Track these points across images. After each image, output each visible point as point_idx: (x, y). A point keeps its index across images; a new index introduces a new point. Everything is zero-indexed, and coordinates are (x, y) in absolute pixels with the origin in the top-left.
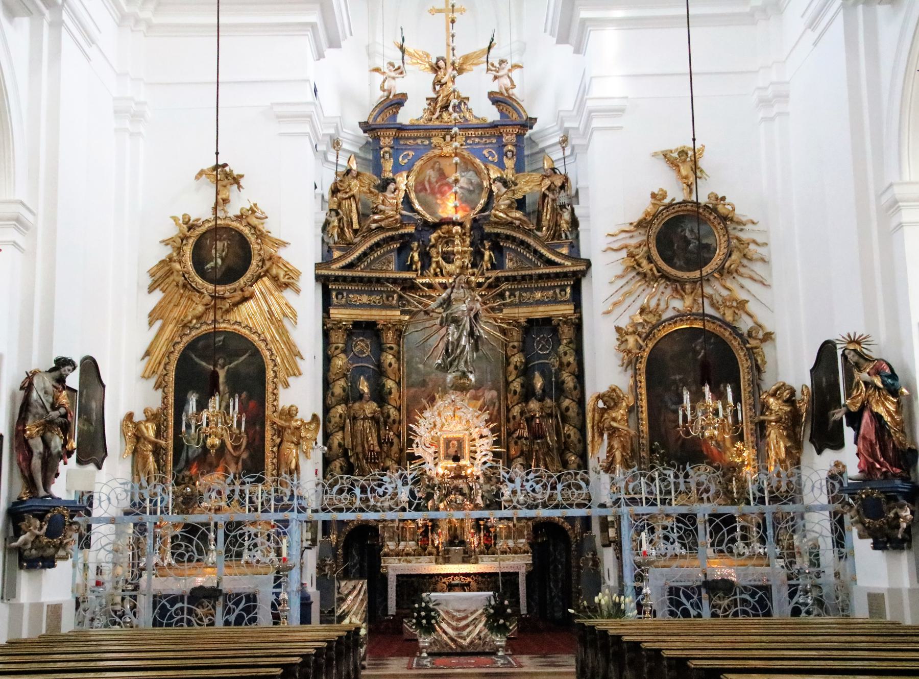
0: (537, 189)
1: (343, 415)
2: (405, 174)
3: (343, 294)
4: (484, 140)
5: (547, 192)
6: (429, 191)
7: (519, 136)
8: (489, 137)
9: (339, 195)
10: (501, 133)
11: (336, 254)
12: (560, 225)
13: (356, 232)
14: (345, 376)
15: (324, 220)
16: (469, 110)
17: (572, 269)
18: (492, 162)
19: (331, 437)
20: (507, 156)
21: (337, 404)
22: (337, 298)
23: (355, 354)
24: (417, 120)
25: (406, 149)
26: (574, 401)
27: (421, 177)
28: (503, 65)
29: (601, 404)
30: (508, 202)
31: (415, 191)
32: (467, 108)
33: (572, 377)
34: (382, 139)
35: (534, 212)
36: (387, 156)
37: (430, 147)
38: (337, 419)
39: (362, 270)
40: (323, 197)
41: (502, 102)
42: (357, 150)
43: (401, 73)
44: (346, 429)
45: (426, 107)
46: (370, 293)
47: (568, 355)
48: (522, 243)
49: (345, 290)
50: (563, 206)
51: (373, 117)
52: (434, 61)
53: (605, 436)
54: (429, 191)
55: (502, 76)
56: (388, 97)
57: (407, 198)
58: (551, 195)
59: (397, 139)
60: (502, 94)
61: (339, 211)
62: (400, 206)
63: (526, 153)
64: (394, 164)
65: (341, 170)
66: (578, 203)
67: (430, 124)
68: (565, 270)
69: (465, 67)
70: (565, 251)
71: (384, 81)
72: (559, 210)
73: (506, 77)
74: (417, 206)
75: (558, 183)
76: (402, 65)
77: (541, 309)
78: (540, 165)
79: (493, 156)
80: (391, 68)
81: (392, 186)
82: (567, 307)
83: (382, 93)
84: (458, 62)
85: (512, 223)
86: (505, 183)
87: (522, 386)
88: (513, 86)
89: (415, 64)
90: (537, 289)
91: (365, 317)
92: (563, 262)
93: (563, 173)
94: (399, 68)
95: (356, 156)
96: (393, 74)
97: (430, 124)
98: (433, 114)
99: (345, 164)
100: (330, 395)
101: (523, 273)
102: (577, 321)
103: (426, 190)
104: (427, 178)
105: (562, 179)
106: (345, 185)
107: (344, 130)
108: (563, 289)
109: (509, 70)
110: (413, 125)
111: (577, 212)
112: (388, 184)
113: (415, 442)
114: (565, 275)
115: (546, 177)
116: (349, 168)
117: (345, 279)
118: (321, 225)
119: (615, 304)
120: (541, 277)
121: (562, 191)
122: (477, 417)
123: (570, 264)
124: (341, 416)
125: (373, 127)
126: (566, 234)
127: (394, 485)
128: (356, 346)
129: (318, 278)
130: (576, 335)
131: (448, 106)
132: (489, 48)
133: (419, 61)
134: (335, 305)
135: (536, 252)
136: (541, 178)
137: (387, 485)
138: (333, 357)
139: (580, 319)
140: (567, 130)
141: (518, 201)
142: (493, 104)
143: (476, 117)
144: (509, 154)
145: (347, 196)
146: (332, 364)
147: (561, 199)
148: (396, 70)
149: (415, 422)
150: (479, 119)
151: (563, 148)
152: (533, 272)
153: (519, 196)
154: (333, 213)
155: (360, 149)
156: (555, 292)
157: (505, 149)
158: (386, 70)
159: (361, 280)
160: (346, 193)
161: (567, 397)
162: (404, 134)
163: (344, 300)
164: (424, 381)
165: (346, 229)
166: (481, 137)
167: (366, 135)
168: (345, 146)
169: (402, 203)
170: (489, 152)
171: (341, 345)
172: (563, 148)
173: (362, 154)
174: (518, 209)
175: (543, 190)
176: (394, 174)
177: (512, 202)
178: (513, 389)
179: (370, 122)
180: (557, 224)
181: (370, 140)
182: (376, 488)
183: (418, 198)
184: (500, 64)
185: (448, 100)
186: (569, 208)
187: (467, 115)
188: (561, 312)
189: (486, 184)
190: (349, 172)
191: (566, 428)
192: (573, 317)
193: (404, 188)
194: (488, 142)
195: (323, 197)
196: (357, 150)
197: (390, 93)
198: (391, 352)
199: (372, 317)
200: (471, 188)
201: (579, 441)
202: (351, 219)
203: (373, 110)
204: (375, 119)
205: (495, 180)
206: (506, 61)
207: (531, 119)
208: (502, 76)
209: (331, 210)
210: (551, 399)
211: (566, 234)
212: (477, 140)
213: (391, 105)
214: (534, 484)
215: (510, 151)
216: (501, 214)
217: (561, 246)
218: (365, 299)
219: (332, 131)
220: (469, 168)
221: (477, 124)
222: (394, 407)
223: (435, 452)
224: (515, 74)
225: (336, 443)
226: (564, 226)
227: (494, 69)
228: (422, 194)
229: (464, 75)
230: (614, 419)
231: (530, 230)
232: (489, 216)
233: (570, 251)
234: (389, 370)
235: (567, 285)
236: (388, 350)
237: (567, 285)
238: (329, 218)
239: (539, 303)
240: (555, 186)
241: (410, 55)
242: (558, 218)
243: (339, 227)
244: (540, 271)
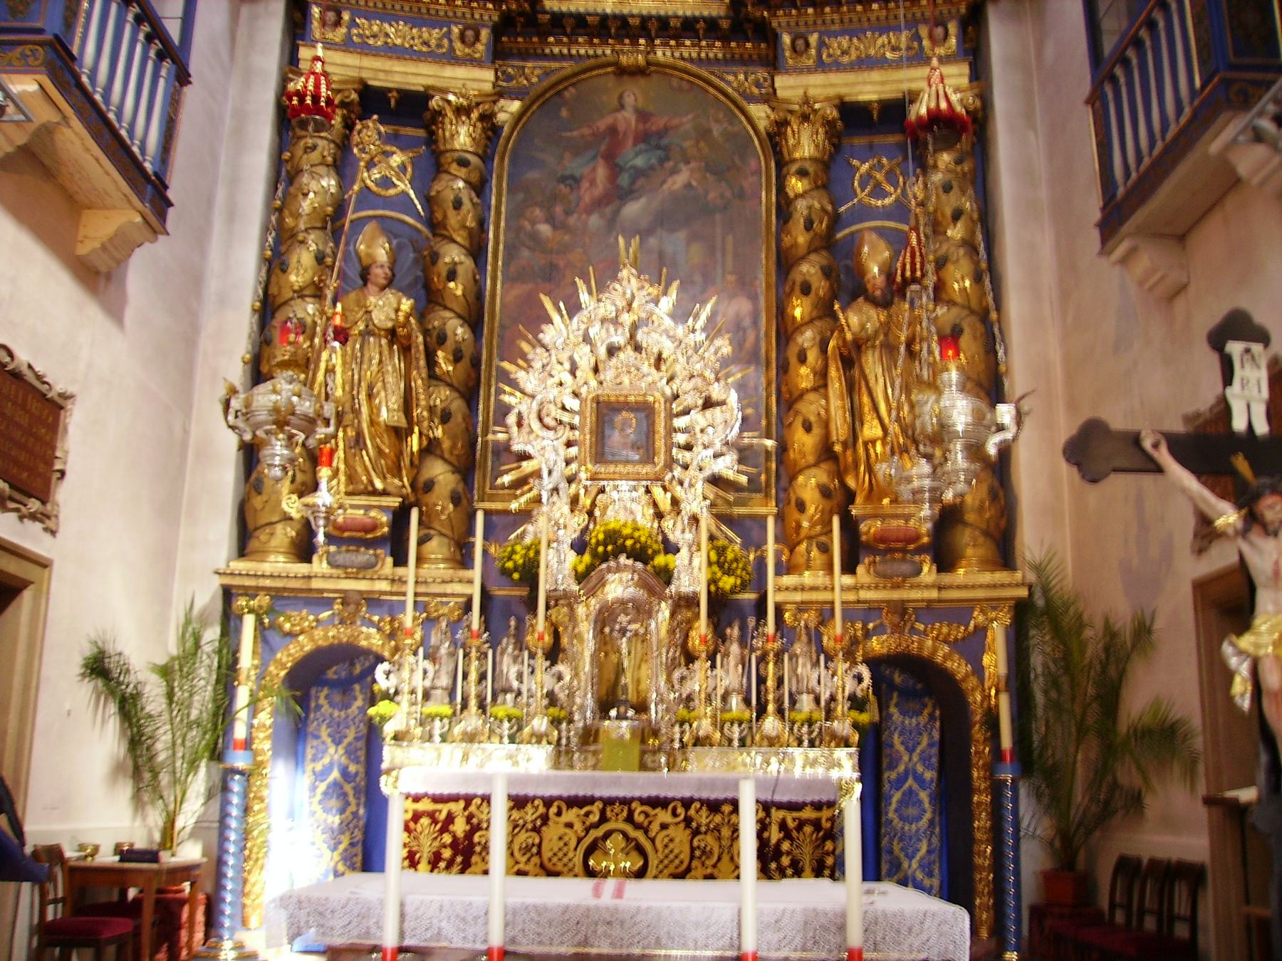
87: (827, 272)
91: (398, 78)
164: (552, 267)
178: (799, 279)
198: (462, 172)
222: (459, 316)
234: (453, 219)
236: (454, 168)
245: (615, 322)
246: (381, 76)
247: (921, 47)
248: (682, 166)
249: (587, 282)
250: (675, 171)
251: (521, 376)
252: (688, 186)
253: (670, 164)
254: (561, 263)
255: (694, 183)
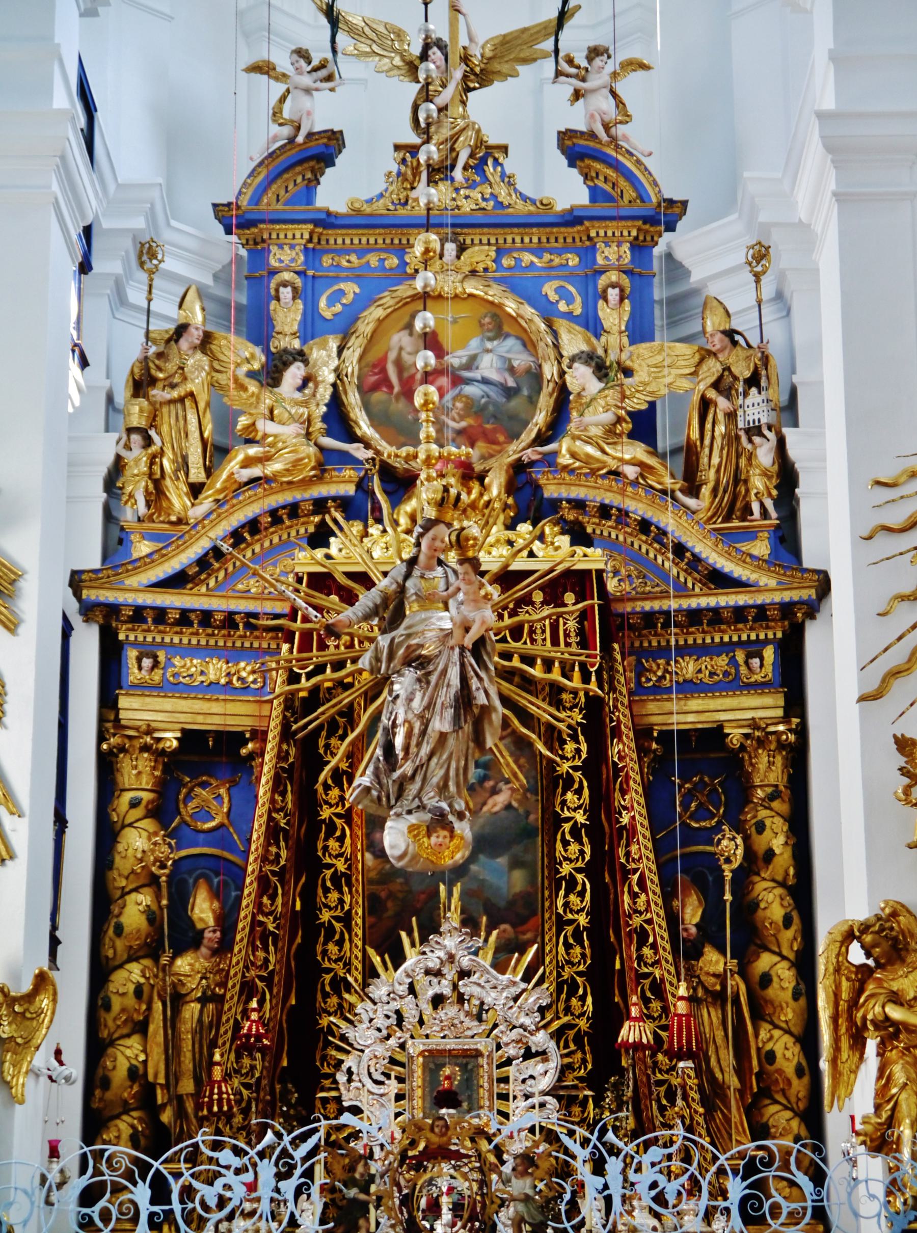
0: (686, 384)
1: (146, 989)
2: (333, 344)
3: (155, 657)
4: (547, 256)
5: (712, 394)
6: (397, 389)
7: (641, 247)
8: (559, 252)
9: (158, 393)
10: (590, 238)
11: (142, 548)
12: (746, 481)
13: (196, 490)
14: (153, 881)
15: (110, 459)
16: (508, 180)
17: (777, 597)
18: (569, 316)
19: (111, 1051)
20: (606, 301)
21: (130, 960)
22: (140, 668)
23: (184, 822)
24: (370, 201)
25: (337, 279)
26: (784, 958)
27: (373, 357)
28: (598, 62)
29: (856, 955)
30: (609, 417)
31: (359, 388)
32: (503, 175)
33: (779, 891)
34: (274, 249)
35: (675, 452)
36: (286, 293)
37: (405, 275)
38: (131, 1001)
39: (210, 593)
40: (110, 399)
41: (595, 158)
42: (208, 280)
43: (329, 78)
44: (151, 1028)
45: (394, 168)
46: (231, 655)
47: (767, 833)
48: (644, 526)
49: (162, 645)
50: (754, 431)
51: (249, 192)
52: (416, 50)
53: (871, 1046)
54: (397, 389)
55: (593, 91)
56: (291, 140)
57: (336, 405)
58: (723, 404)
59: (312, 252)
60: (592, 135)
61: (152, 433)
62: (318, 425)
63: (659, 292)
64: (304, 314)
65: (163, 327)
66: (796, 424)
67: (402, 211)
68: (760, 599)
69: (496, 66)
70: (761, 548)
71: (283, 99)
72: (744, 439)
73: (606, 91)
74: (364, 427)
75: (743, 371)
76: (329, 55)
77: (695, 704)
78: (694, 327)
79: (570, 301)
80: (302, 63)
81: (294, 374)
82: (768, 700)
83: (275, 129)
84: (476, 52)
85: (615, 473)
86: (601, 370)
88: (626, 117)
89: (366, 54)
90: (684, 651)
91: (217, 720)
92: (753, 577)
93: (754, 342)
94: (322, 66)
95: (202, 294)
96: (307, 80)
97: (402, 211)
98: (413, 188)
99: (173, 311)
100: (111, 932)
101: (647, 606)
102: (792, 737)
103: (391, 387)
104: (392, 356)
105: (756, 359)
106: (171, 367)
107: (174, 223)
108: (754, 650)
109: (615, 75)
110: (358, 212)
111: (793, 452)
112: (286, 365)
113: (344, 1067)
114: (761, 613)
115: (706, 354)
116: (183, 321)
117: (160, 615)
118: (103, 471)
119: (895, 673)
120: (694, 617)
121: (754, 390)
122: (516, 999)
123: (772, 583)
124: (139, 991)
125: (249, 216)
126: (762, 505)
127: (249, 1177)
128: (188, 797)
129: (88, 610)
130: (790, 776)
131: (453, 167)
132: (563, 17)
133: (375, 47)
134: (134, 686)
135: (680, 550)
136: (697, 357)
137: (229, 1177)
138: (124, 827)
139: (802, 732)
140: (766, 228)
141: (634, 416)
142: (572, 164)
143: (525, 198)
144: (613, 294)
145: (175, 394)
146: (120, 847)
147: (749, 411)
148: (315, 70)
149: (345, 1011)
150: (533, 202)
151: (757, 277)
152: (673, 604)
153: (638, 403)
154: (136, 438)
155: (216, 277)
156: (733, 661)
157: (602, 281)
158: (289, 70)
159: (206, 617)
160: (173, 386)
161: (767, 949)
162: (337, 238)
163: (157, 676)
165: (168, 482)
166: (538, 251)
167: (234, 238)
168: (170, 264)
169: (325, 418)
170: (559, 290)
171: (146, 796)
172: (757, 277)
173: (220, 292)
174: (632, 435)
175: (702, 386)
176: (304, 341)
177: (619, 420)
179: (244, 202)
180: (738, 479)
181: (243, 252)
182: (196, 1184)
183: (367, 407)
184: (590, 59)
185: (452, 149)
186: (771, 435)
187: (503, 193)
188: (749, 715)
189: (549, 370)
190: (181, 330)
191: (763, 1035)
192: (781, 728)
193: (331, 378)
194: (557, 261)
195: (110, 399)
196: (208, 280)
197: (298, 128)
199: (230, 721)
200: (511, 383)
201: (799, 1072)
202: (185, 459)
203: (252, 174)
204: (256, 200)
205: (573, 359)
206: (606, 50)
207: (671, 202)
208: (593, 91)
209: (130, 431)
210: (723, 952)
211: (762, 505)
212: (527, 258)
213: (300, 162)
214: (662, 1180)
215: (613, 286)
216: (590, 450)
217: (750, 535)
218: (216, 670)
219: (139, 223)
220: (506, 328)
221: (530, 214)
223: (399, 1097)
224: (628, 87)
225: (122, 1067)
226: (758, 483)
227: (573, 71)
228: (378, 396)
229: (497, 88)
230: (896, 998)
231: (664, 492)
232: (555, 454)
233: (774, 553)
235: (766, 642)
237: (766, 642)
238: (124, 453)
239: (689, 688)
240: (736, 378)
241: (353, 31)
242: (743, 462)
243: (150, 475)
244: (693, 603)
245: (438, 974)
246: (200, 719)
247: (737, 671)
248: (501, 785)
249: (410, 934)
250: (495, 791)
251: (351, 1034)
252: (508, 807)
253: (489, 784)
254: (383, 895)
255: (515, 804)
